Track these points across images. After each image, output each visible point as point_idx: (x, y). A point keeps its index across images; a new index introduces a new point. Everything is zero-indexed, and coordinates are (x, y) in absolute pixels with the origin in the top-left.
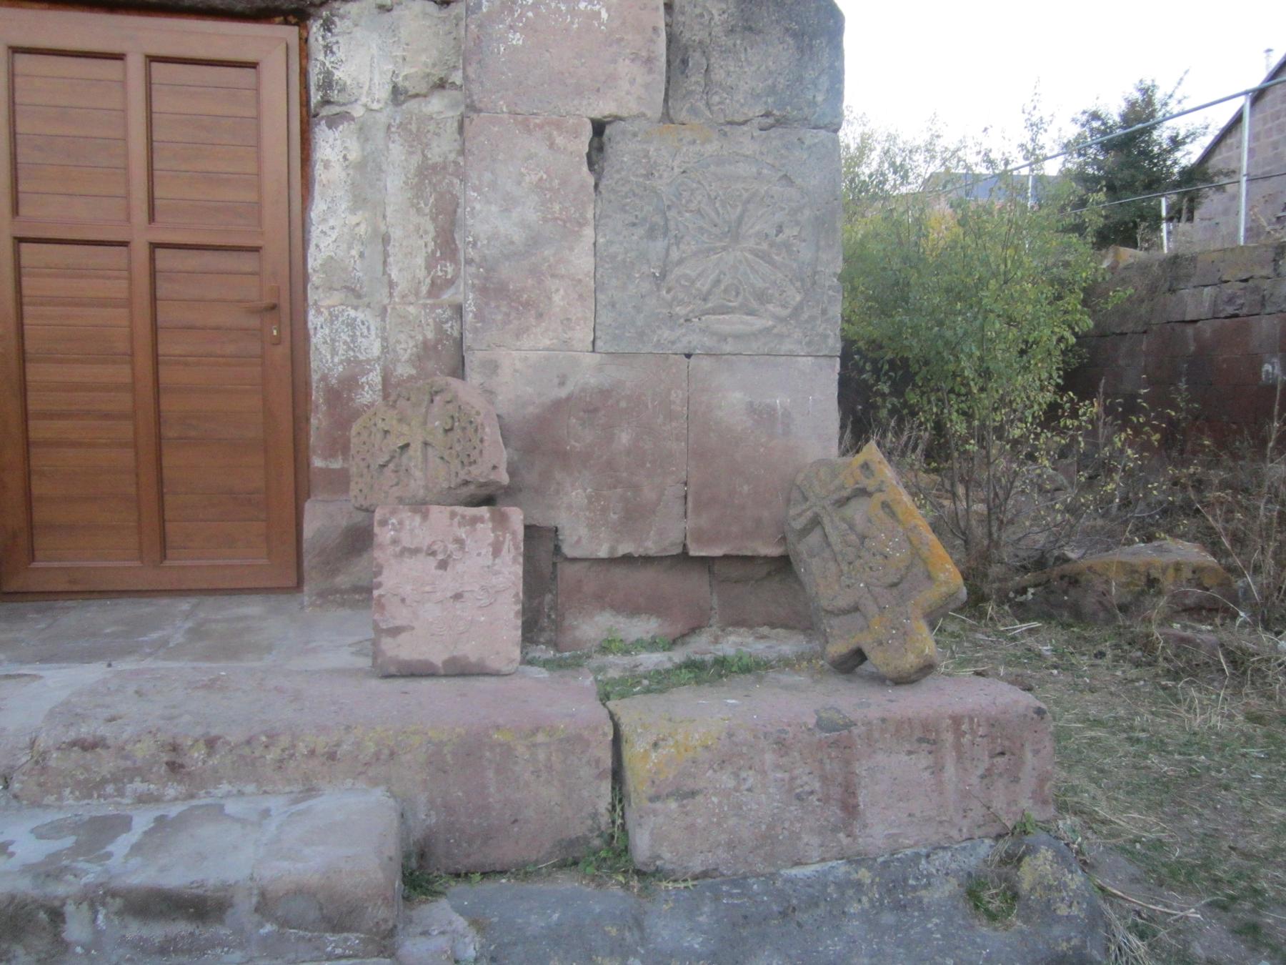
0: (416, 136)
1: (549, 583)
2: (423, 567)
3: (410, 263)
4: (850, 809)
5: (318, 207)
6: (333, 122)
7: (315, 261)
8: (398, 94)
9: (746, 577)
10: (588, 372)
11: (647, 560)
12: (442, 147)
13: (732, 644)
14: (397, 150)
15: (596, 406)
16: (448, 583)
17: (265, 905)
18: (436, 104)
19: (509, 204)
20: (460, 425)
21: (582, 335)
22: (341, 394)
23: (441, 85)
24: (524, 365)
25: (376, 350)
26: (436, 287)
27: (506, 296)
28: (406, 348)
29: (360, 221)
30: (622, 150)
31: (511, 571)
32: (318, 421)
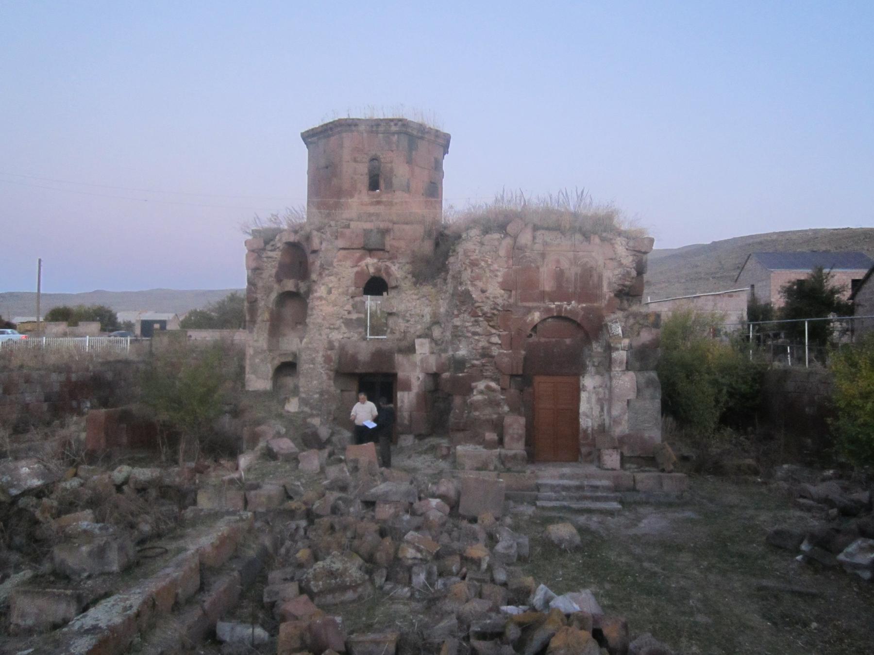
0: (597, 394)
1: (623, 460)
4: (661, 485)
5: (581, 403)
8: (594, 388)
9: (648, 459)
10: (627, 432)
12: (601, 396)
13: (647, 469)
15: (629, 436)
17: (603, 487)
18: (600, 389)
20: (612, 439)
22: (585, 431)
23: (601, 386)
24: (619, 431)
25: (590, 424)
28: (596, 425)
31: (619, 457)
32: (581, 435)
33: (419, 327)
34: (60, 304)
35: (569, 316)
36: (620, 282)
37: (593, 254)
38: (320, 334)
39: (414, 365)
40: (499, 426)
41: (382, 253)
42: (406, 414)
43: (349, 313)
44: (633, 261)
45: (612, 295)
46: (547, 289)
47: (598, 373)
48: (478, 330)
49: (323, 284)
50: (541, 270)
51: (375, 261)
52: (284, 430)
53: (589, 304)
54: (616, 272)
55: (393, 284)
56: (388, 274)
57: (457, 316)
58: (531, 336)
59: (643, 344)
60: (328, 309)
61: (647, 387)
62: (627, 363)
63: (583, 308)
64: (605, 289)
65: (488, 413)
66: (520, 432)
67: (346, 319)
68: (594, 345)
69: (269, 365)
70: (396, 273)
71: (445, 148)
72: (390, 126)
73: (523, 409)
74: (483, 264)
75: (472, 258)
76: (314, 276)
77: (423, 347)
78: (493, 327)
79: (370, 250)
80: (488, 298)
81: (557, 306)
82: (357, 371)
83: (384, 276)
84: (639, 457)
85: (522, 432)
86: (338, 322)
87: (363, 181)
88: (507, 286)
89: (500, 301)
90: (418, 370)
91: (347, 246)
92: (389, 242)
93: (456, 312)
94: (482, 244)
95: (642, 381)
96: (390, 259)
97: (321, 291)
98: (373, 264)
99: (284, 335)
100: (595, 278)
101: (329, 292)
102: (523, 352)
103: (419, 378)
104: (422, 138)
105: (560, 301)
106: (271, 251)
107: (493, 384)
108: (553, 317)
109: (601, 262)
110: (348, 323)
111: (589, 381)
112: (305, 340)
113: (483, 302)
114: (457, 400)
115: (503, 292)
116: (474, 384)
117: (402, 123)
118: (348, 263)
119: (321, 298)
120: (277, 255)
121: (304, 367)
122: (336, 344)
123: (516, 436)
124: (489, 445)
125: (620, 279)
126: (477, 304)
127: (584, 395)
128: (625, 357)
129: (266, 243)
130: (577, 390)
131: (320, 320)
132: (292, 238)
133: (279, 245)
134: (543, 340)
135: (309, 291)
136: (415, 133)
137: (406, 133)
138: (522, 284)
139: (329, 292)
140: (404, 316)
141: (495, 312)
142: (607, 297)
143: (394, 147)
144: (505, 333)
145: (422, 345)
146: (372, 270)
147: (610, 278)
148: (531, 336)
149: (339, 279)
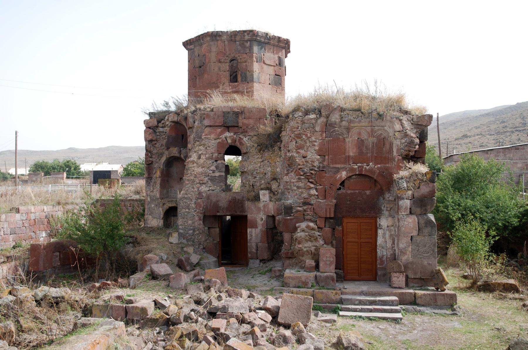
0: (390, 231)
2: (396, 278)
3: (389, 245)
4: (436, 301)
5: (378, 238)
6: (380, 229)
7: (378, 244)
8: (388, 226)
10: (411, 259)
11: (417, 278)
12: (393, 233)
14: (387, 232)
15: (412, 263)
16: (398, 280)
18: (392, 228)
19: (403, 244)
21: (410, 256)
24: (404, 259)
26: (392, 248)
27: (403, 252)
28: (389, 254)
29: (383, 240)
30: (414, 239)
31: (404, 279)
33: (263, 182)
34: (40, 159)
35: (368, 174)
36: (406, 148)
37: (386, 128)
38: (193, 188)
39: (259, 210)
40: (316, 256)
41: (236, 128)
42: (254, 245)
43: (214, 172)
44: (417, 132)
45: (400, 158)
46: (351, 154)
47: (390, 216)
48: (301, 184)
49: (195, 152)
50: (347, 140)
51: (232, 134)
52: (166, 257)
53: (382, 165)
54: (403, 141)
55: (245, 151)
56: (241, 143)
57: (287, 174)
58: (340, 189)
59: (423, 194)
60: (200, 170)
61: (426, 226)
62: (410, 208)
63: (378, 168)
64: (395, 154)
65: (308, 246)
66: (332, 259)
67: (211, 176)
68: (387, 195)
69: (161, 209)
70: (247, 142)
71: (287, 50)
72: (244, 36)
73: (334, 242)
74: (304, 137)
75: (296, 133)
76: (189, 146)
77: (264, 196)
78: (311, 183)
79: (228, 128)
80: (307, 162)
81: (359, 167)
82: (218, 214)
83: (238, 144)
84: (421, 279)
85: (333, 259)
86: (206, 179)
87: (225, 77)
88: (321, 153)
89: (316, 164)
90: (262, 213)
91: (211, 124)
92: (242, 121)
93: (286, 172)
94: (303, 122)
95: (422, 222)
96: (242, 133)
97: (194, 157)
98: (230, 137)
99: (172, 187)
100: (387, 146)
101: (199, 158)
102: (335, 201)
103: (262, 219)
104: (268, 43)
105: (362, 163)
106: (162, 127)
107: (312, 224)
108: (356, 175)
109: (391, 134)
110: (213, 179)
111: (384, 222)
112: (182, 192)
113: (303, 165)
114: (286, 236)
115: (319, 157)
116: (297, 225)
117: (251, 33)
118: (213, 136)
119: (193, 162)
120: (167, 129)
121: (181, 211)
122: (204, 195)
123: (328, 263)
124: (309, 269)
125: (406, 146)
126: (299, 167)
127: (380, 232)
128: (409, 204)
129: (159, 122)
130: (375, 228)
131: (192, 178)
132: (176, 119)
133: (167, 123)
134: (349, 192)
135: (186, 157)
136: (263, 40)
137: (256, 40)
138: (332, 150)
139: (199, 158)
140: (252, 174)
141: (313, 172)
142: (396, 160)
143: (248, 51)
144: (320, 187)
145: (264, 195)
146: (229, 141)
147: (398, 145)
148: (340, 189)
149: (206, 148)
